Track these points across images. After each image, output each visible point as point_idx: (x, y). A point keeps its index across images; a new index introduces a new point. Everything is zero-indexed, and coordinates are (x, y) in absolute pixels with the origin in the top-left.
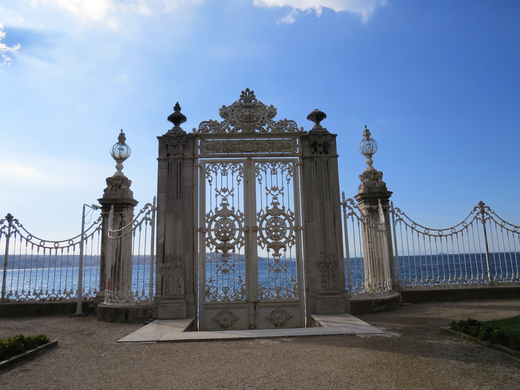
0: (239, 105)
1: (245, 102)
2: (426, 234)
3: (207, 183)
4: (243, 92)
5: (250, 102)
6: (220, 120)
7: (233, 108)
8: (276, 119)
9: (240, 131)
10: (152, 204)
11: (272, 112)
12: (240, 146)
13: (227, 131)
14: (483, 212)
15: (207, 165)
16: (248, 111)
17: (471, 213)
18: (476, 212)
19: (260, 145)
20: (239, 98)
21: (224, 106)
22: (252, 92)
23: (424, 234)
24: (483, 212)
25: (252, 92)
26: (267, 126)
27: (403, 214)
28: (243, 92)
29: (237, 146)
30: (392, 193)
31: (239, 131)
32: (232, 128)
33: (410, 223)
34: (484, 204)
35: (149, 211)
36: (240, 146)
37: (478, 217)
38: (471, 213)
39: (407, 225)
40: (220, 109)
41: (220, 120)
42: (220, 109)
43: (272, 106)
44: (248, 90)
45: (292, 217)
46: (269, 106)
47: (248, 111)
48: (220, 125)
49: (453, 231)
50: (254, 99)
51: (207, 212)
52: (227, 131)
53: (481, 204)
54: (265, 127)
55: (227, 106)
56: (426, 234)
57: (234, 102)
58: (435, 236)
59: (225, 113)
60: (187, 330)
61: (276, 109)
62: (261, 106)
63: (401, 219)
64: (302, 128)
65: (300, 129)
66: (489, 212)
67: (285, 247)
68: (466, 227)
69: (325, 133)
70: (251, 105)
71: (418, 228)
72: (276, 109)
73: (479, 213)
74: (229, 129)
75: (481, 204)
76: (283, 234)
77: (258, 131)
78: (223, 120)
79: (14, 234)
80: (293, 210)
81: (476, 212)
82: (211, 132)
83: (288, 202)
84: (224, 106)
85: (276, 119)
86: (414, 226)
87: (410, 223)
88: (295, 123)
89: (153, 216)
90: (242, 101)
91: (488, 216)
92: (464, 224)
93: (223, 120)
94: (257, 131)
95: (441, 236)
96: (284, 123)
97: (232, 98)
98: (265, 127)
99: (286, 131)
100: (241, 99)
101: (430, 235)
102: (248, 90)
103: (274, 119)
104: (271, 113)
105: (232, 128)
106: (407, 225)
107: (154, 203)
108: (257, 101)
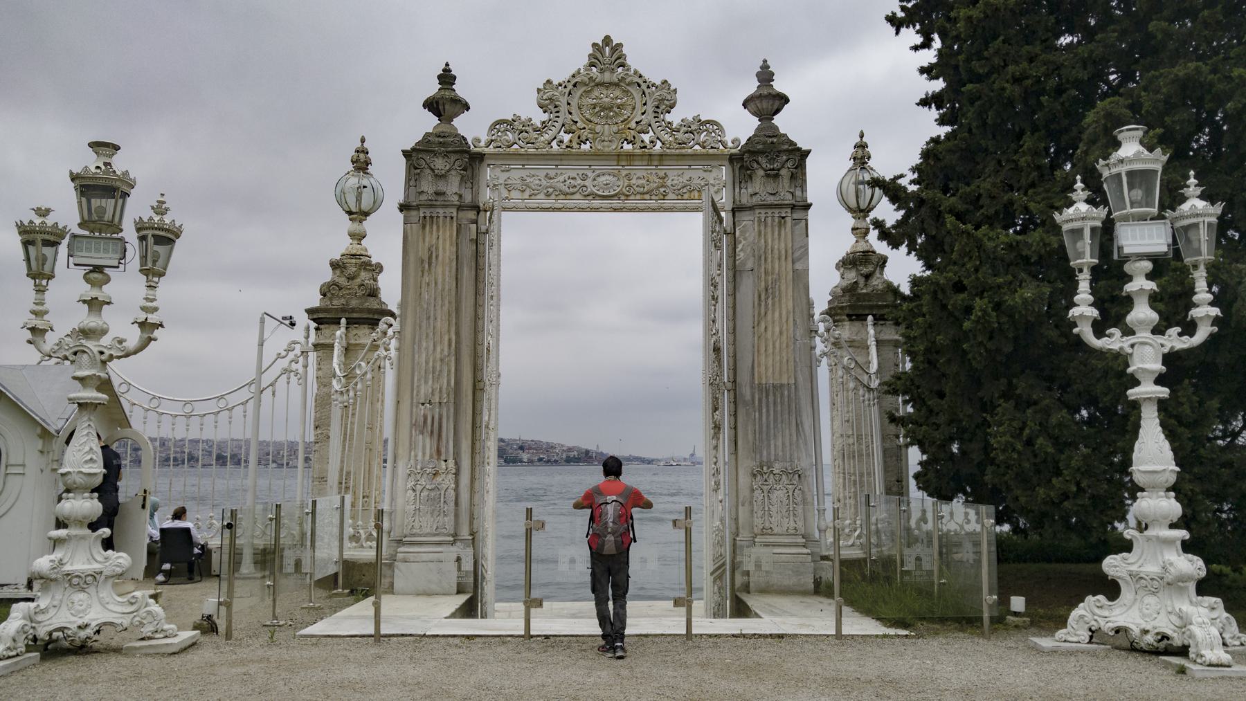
1: (602, 71)
6: (539, 117)
7: (570, 87)
9: (586, 147)
11: (665, 100)
12: (586, 183)
13: (554, 144)
20: (586, 61)
21: (549, 82)
26: (651, 133)
29: (579, 181)
31: (583, 146)
36: (586, 183)
40: (539, 90)
41: (539, 117)
42: (539, 90)
44: (607, 40)
52: (554, 144)
54: (646, 138)
55: (556, 82)
57: (573, 71)
62: (640, 83)
74: (562, 142)
78: (545, 117)
82: (515, 146)
84: (549, 82)
90: (594, 69)
93: (545, 117)
94: (627, 147)
97: (571, 60)
98: (646, 138)
99: (697, 147)
100: (592, 65)
102: (607, 40)
105: (567, 138)
108: (629, 70)
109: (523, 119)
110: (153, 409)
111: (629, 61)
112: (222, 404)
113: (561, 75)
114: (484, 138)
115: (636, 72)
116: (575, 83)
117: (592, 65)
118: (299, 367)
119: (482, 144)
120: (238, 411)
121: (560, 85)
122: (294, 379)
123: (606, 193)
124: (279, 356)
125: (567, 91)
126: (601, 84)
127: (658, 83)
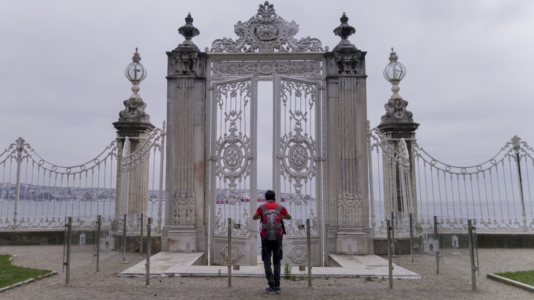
0: (257, 20)
1: (264, 17)
2: (448, 171)
3: (218, 107)
4: (261, 6)
5: (269, 17)
6: (235, 38)
7: (249, 24)
8: (298, 37)
9: (257, 51)
10: (162, 129)
13: (242, 50)
14: (516, 148)
15: (219, 87)
16: (265, 26)
17: (503, 149)
18: (508, 149)
19: (279, 67)
20: (257, 12)
21: (240, 22)
22: (272, 6)
23: (445, 172)
24: (516, 148)
25: (272, 6)
26: (287, 44)
27: (422, 149)
28: (261, 6)
29: (254, 68)
30: (419, 125)
31: (256, 51)
32: (248, 47)
33: (429, 160)
34: (520, 139)
35: (159, 137)
37: (511, 154)
38: (503, 149)
39: (425, 161)
40: (235, 26)
41: (235, 38)
42: (235, 26)
43: (293, 22)
44: (266, 3)
45: (313, 145)
46: (290, 22)
47: (265, 26)
48: (233, 44)
49: (479, 168)
50: (274, 14)
51: (218, 139)
52: (242, 50)
53: (516, 140)
54: (285, 46)
55: (243, 22)
56: (448, 171)
58: (458, 174)
59: (240, 30)
60: (195, 264)
61: (298, 25)
63: (419, 155)
64: (327, 48)
65: (324, 49)
66: (525, 148)
67: (305, 178)
68: (496, 165)
69: (353, 51)
70: (270, 20)
71: (438, 165)
72: (298, 25)
73: (512, 149)
74: (245, 49)
75: (516, 140)
76: (304, 163)
77: (277, 50)
79: (26, 158)
80: (314, 138)
81: (508, 149)
82: (225, 51)
83: (309, 130)
84: (240, 22)
85: (298, 37)
86: (433, 162)
87: (429, 160)
88: (319, 42)
89: (163, 142)
90: (260, 16)
91: (524, 153)
92: (493, 162)
94: (276, 51)
95: (464, 174)
96: (307, 41)
97: (249, 12)
99: (309, 50)
100: (259, 14)
101: (451, 173)
102: (266, 3)
103: (295, 37)
104: (292, 30)
105: (248, 47)
106: (425, 161)
107: (164, 128)
108: (277, 16)
109: (228, 38)
110: (54, 171)
111: (276, 12)
112: (83, 168)
113: (245, 19)
114: (210, 48)
115: (280, 17)
116: (253, 22)
117: (259, 14)
118: (116, 152)
119: (209, 50)
120: (90, 171)
121: (245, 23)
122: (114, 157)
123: (266, 73)
124: (108, 148)
125: (248, 26)
126: (263, 23)
127: (290, 22)
